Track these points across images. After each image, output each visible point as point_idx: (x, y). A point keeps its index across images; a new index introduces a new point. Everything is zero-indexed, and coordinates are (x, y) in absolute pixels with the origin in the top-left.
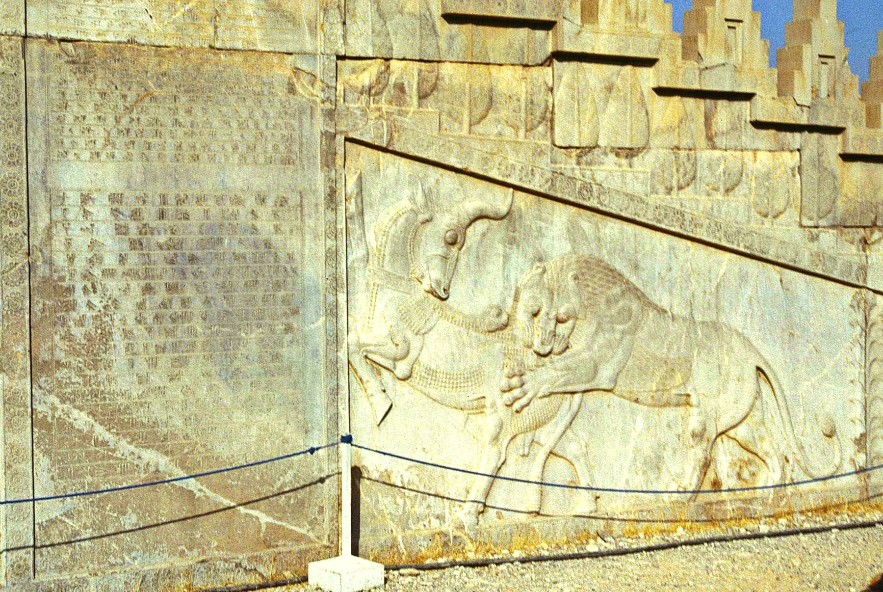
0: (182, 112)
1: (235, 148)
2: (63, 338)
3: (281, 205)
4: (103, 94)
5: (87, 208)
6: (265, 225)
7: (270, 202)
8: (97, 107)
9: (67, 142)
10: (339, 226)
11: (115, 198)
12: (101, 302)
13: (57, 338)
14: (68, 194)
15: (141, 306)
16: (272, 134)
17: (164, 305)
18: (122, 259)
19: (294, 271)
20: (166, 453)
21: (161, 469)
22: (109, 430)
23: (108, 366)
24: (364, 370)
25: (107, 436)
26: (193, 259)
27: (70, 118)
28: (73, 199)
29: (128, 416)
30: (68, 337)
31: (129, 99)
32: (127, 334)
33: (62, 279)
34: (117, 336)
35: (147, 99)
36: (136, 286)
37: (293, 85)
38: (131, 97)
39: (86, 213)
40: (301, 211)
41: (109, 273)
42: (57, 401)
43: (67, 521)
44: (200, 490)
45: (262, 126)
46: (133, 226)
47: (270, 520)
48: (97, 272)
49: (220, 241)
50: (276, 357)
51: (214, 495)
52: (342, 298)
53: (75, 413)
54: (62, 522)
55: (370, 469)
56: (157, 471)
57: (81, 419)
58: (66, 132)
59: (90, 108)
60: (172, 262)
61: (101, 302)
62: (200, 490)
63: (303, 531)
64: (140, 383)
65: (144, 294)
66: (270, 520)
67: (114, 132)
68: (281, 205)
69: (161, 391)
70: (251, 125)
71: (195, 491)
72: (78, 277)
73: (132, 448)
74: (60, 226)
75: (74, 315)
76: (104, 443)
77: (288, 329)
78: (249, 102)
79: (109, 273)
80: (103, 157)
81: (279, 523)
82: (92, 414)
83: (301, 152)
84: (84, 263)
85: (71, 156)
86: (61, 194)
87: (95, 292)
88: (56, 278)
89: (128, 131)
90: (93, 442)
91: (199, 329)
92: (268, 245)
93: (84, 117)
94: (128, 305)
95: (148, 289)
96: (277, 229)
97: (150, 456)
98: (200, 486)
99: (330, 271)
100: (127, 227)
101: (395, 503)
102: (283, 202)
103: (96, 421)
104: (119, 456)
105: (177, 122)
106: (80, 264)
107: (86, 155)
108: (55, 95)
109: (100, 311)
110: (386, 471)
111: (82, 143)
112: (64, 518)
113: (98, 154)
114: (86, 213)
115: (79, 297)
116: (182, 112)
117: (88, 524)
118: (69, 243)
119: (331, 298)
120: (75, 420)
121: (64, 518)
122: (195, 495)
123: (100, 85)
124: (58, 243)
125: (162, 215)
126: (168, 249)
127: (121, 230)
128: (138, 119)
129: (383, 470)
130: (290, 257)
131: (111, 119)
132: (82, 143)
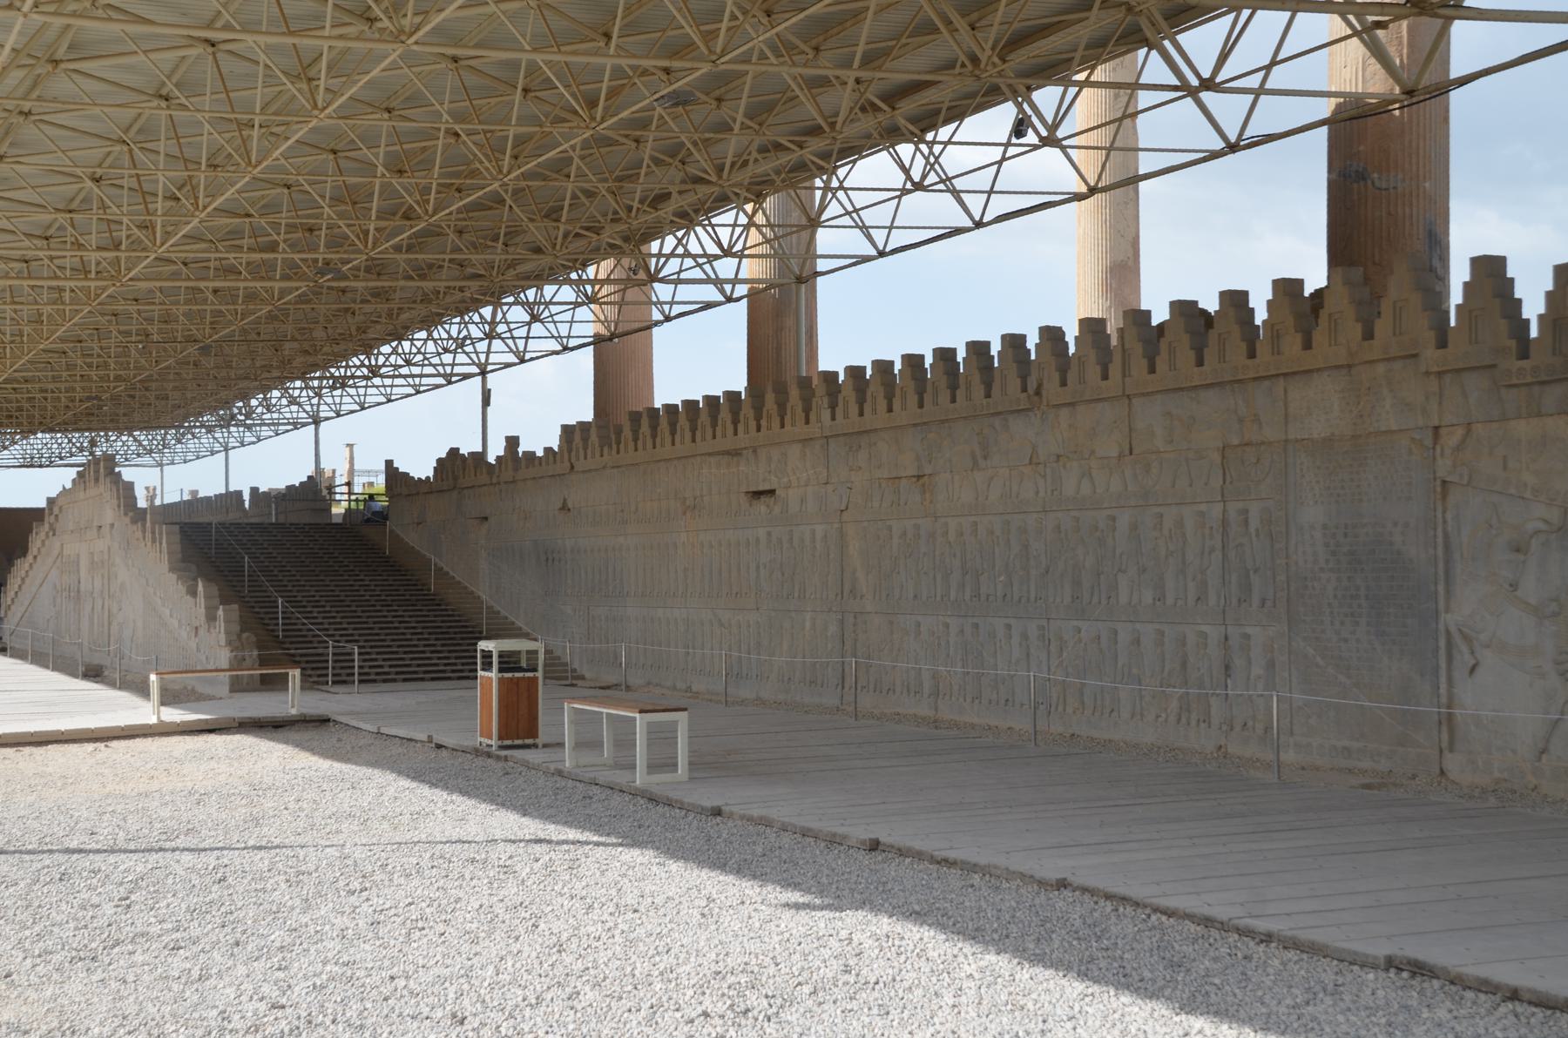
18: (1327, 561)
32: (1329, 604)
39: (1312, 537)
41: (1322, 569)
53: (1308, 648)
69: (1346, 640)
79: (1322, 569)
127: (1327, 545)
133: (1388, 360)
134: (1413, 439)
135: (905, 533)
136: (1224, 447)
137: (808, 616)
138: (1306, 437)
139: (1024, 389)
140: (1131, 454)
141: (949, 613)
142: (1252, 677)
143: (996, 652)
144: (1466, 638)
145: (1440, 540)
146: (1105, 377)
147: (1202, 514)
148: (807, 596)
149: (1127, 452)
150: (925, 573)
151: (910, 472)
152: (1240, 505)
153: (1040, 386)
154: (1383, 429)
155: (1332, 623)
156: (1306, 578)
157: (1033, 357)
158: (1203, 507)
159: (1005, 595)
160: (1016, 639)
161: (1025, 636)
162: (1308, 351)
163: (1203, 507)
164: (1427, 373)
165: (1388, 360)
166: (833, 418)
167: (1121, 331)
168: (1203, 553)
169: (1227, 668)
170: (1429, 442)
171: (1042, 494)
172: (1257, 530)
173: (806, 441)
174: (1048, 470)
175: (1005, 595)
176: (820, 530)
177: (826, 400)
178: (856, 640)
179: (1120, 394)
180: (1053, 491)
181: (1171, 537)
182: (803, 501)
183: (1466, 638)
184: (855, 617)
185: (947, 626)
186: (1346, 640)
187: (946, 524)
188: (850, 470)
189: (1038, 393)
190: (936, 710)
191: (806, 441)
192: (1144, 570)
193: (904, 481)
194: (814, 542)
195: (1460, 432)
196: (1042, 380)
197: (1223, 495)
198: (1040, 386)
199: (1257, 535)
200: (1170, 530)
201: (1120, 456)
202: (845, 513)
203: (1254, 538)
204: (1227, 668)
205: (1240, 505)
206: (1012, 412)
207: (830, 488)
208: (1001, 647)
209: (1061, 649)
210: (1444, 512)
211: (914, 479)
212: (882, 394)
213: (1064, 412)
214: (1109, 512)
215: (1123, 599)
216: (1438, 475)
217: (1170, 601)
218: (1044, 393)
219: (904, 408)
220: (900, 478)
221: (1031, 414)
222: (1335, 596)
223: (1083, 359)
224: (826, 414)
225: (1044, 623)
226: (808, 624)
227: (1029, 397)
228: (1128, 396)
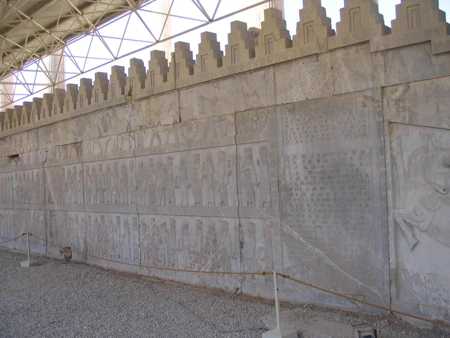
0: (323, 122)
1: (343, 133)
2: (289, 206)
3: (362, 154)
4: (298, 120)
5: (295, 161)
6: (356, 163)
7: (358, 153)
8: (297, 125)
9: (289, 138)
10: (387, 161)
11: (303, 156)
12: (300, 193)
13: (288, 206)
14: (289, 156)
15: (313, 195)
16: (357, 125)
17: (320, 195)
18: (306, 178)
19: (369, 181)
20: (323, 250)
21: (321, 256)
22: (304, 239)
23: (303, 216)
24: (404, 227)
25: (304, 241)
26: (329, 177)
27: (289, 130)
28: (291, 157)
29: (310, 235)
30: (291, 205)
31: (306, 120)
32: (308, 205)
33: (289, 185)
34: (306, 207)
35: (312, 119)
36: (311, 187)
37: (365, 103)
38: (307, 119)
39: (295, 162)
40: (371, 156)
41: (302, 183)
42: (289, 227)
43: (293, 268)
44: (335, 267)
45: (353, 122)
46: (309, 166)
47: (362, 284)
48: (299, 183)
49: (339, 170)
50: (363, 217)
51: (340, 269)
52: (390, 193)
53: (294, 232)
54: (291, 269)
55: (408, 271)
56: (320, 256)
57: (295, 234)
58: (288, 135)
59: (294, 125)
60: (322, 179)
61: (300, 193)
62: (335, 267)
63: (376, 292)
64: (313, 223)
65: (313, 191)
66: (362, 284)
67: (302, 133)
68: (362, 154)
69: (320, 227)
70: (349, 123)
71: (333, 267)
72: (293, 185)
73: (311, 247)
74: (287, 167)
75: (292, 198)
76: (303, 244)
77: (367, 206)
78: (348, 114)
79: (302, 183)
80: (299, 142)
81: (366, 286)
82: (298, 233)
83: (369, 131)
84: (295, 180)
85: (290, 143)
86: (287, 157)
87: (298, 190)
88: (287, 185)
89: (306, 132)
90: (299, 243)
91: (333, 204)
92: (357, 170)
93: (293, 129)
94: (308, 195)
95: (314, 189)
96: (361, 164)
97: (317, 250)
98: (335, 265)
99: (383, 181)
100: (307, 166)
101: (422, 289)
102: (363, 152)
103: (300, 235)
104: (307, 249)
105: (322, 126)
106: (294, 180)
107: (294, 142)
108: (284, 123)
109: (300, 197)
110: (417, 273)
111: (293, 138)
112: (292, 267)
113: (297, 141)
114: (295, 162)
115: (294, 192)
116: (323, 122)
117: (299, 271)
118: (290, 173)
119: (384, 193)
120: (294, 234)
121: (292, 267)
122: (333, 268)
123: (297, 117)
124: (287, 174)
125: (318, 161)
126: (321, 174)
127: (305, 167)
128: (309, 127)
129: (415, 272)
130: (367, 175)
131: (301, 128)
132: (293, 138)
133: (345, 47)
134: (366, 97)
135: (70, 171)
136: (235, 113)
137: (32, 212)
138: (289, 102)
139: (123, 93)
140: (180, 122)
141: (90, 211)
142: (256, 249)
143: (113, 230)
144: (411, 227)
145: (388, 161)
146: (165, 80)
147: (222, 153)
148: (31, 203)
149: (178, 121)
150: (79, 191)
151: (72, 141)
152: (247, 146)
153: (131, 90)
154: (343, 92)
155: (310, 216)
156: (291, 189)
157: (128, 76)
158: (223, 149)
159: (116, 201)
160: (122, 224)
161: (126, 223)
162: (290, 49)
163: (223, 149)
164: (376, 52)
165: (345, 47)
166: (39, 119)
167: (173, 55)
168: (224, 175)
169: (241, 243)
170: (378, 97)
171: (133, 147)
172: (258, 160)
173: (29, 131)
174: (136, 135)
175: (116, 201)
176: (35, 171)
177: (36, 110)
178: (51, 224)
179: (174, 88)
180: (139, 145)
181: (204, 167)
182: (29, 159)
183: (411, 227)
184: (51, 213)
185: (90, 217)
186: (320, 227)
187: (88, 166)
188: (47, 143)
189: (130, 94)
190: (86, 258)
191: (29, 131)
192: (189, 187)
193: (69, 146)
194: (33, 177)
195: (401, 89)
196: (132, 87)
197: (236, 141)
198: (131, 90)
199: (258, 164)
200: (204, 163)
201: (174, 124)
202: (45, 163)
203: (256, 165)
204: (241, 243)
205: (247, 146)
206: (118, 106)
207: (39, 152)
208: (115, 228)
209: (145, 230)
210: (391, 143)
211: (74, 145)
212: (59, 105)
213: (144, 102)
214: (169, 155)
215: (178, 203)
216: (386, 118)
217: (205, 203)
218: (133, 93)
219: (68, 110)
220: (67, 145)
221: (127, 106)
222: (312, 200)
223: (153, 72)
224: (36, 117)
225: (137, 216)
226: (32, 215)
227: (126, 97)
228: (178, 89)
